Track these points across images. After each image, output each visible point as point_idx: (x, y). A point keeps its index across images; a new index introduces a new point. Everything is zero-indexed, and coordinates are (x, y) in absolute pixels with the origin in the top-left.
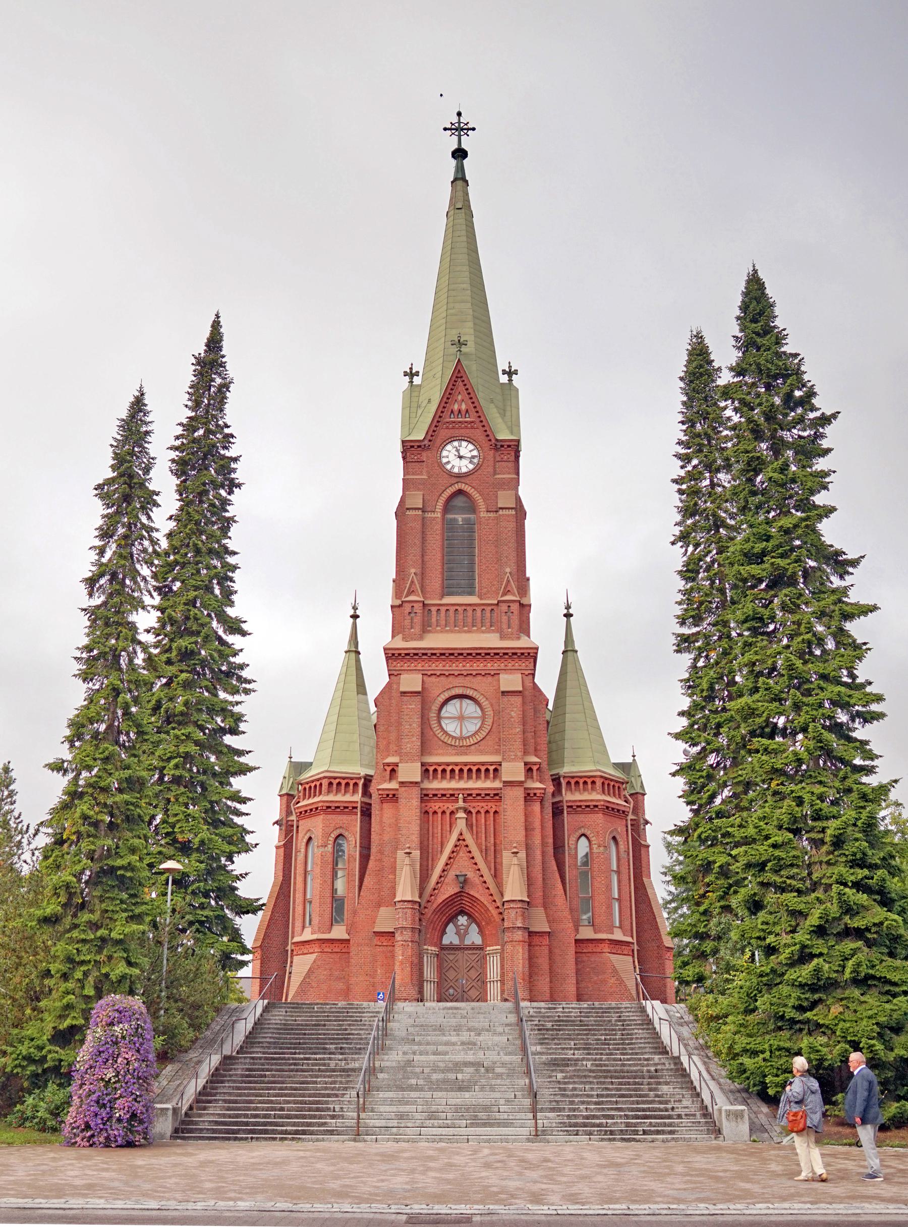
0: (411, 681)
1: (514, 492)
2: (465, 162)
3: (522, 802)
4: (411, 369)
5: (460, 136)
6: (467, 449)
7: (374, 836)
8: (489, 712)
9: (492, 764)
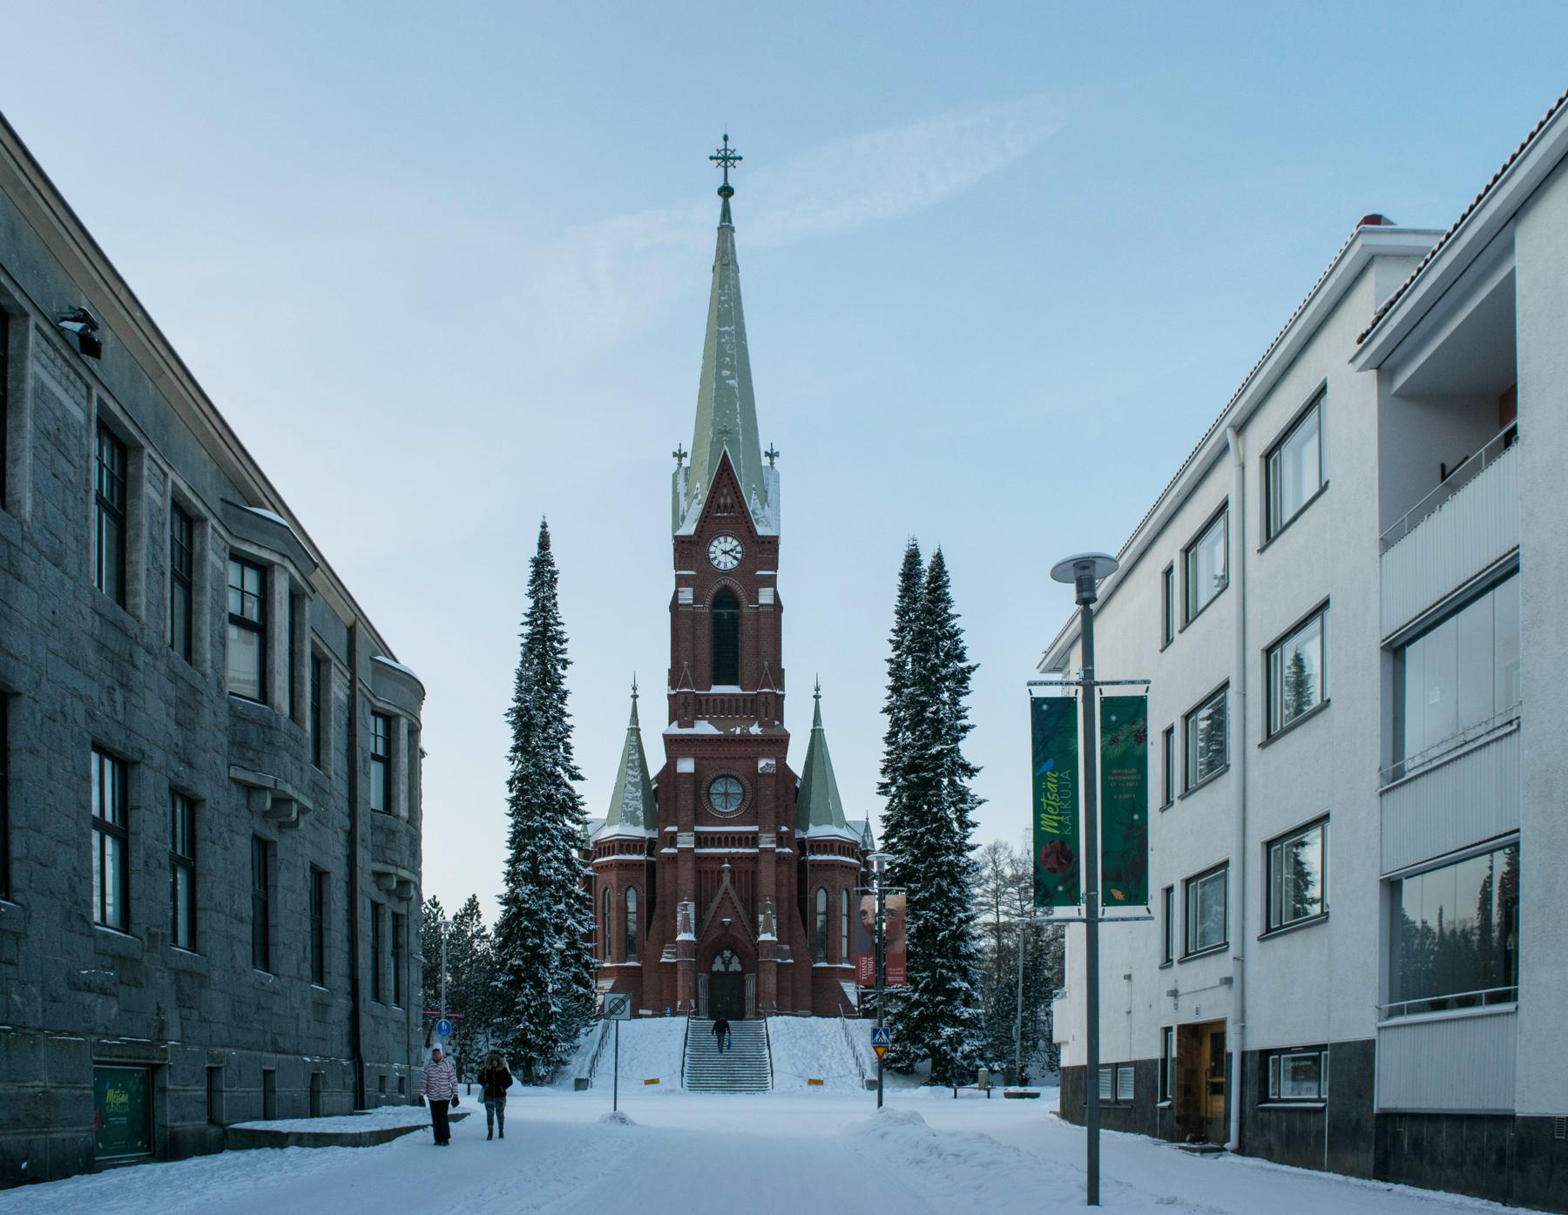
0: (686, 766)
1: (772, 589)
2: (731, 200)
3: (773, 864)
4: (680, 451)
5: (726, 168)
6: (731, 543)
7: (659, 890)
8: (749, 790)
9: (750, 833)
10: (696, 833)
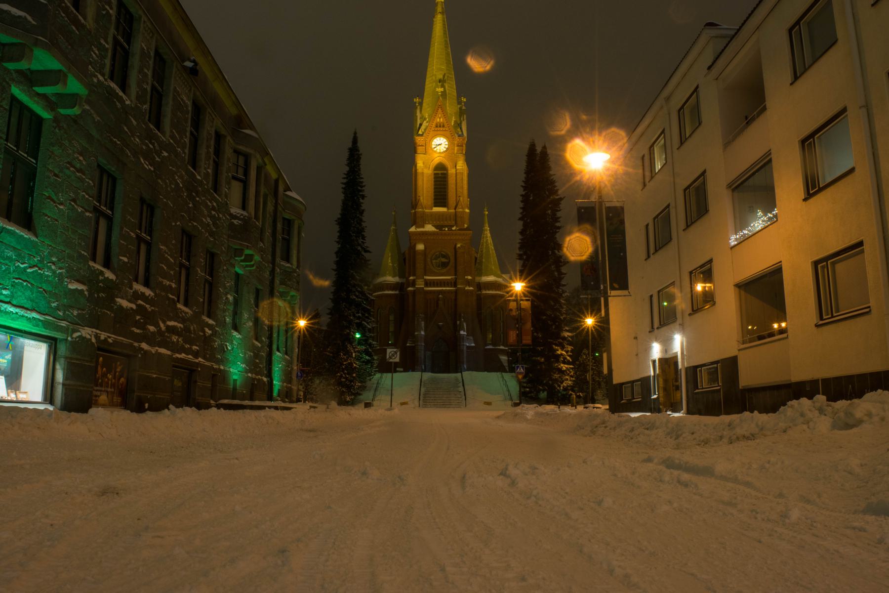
10: (425, 279)
